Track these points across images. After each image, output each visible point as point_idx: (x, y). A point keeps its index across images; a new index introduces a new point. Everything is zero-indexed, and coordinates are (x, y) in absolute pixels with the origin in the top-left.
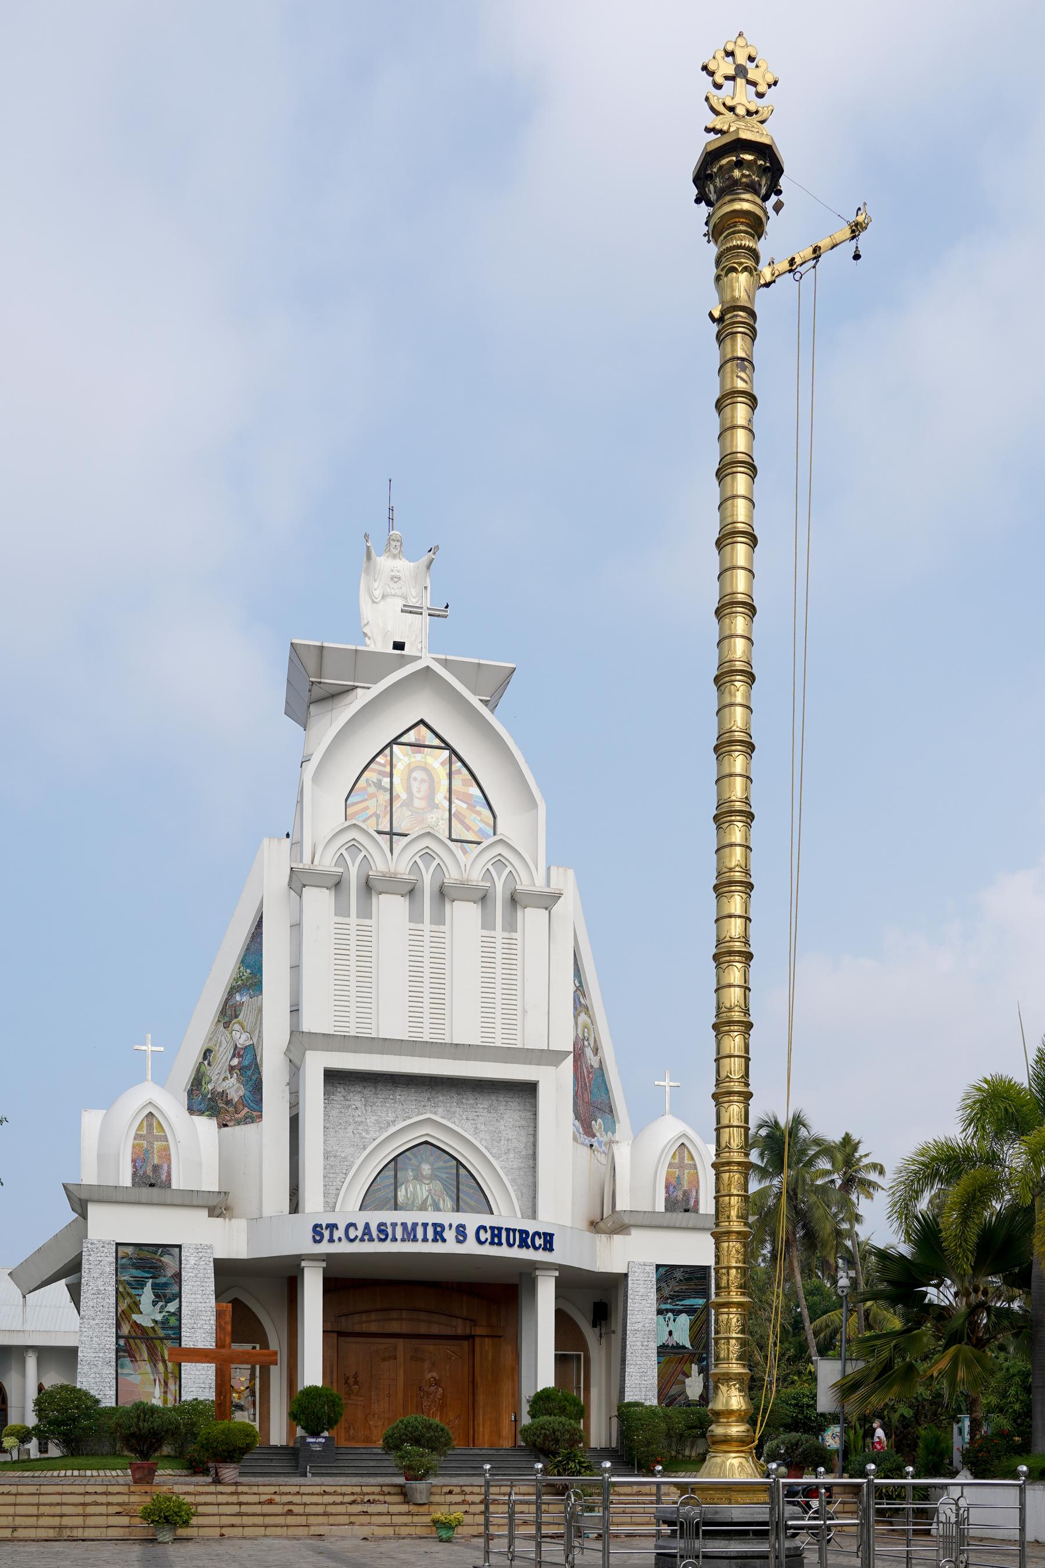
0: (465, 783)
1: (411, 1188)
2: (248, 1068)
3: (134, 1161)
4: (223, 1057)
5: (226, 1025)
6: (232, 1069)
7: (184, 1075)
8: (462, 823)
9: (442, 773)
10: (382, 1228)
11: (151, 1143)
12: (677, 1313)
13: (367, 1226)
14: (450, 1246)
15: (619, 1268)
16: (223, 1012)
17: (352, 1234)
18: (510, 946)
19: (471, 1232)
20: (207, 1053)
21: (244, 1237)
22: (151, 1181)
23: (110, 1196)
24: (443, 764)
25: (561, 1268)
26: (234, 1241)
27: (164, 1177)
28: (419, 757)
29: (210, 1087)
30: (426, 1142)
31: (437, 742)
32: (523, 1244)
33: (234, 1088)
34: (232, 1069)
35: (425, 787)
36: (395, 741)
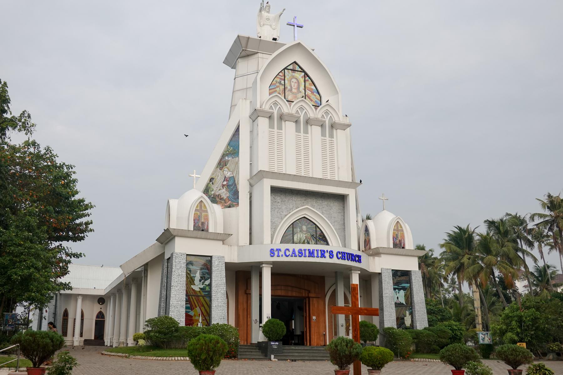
0: (310, 84)
1: (299, 235)
2: (231, 185)
3: (194, 220)
4: (219, 181)
5: (221, 169)
6: (223, 186)
7: (203, 187)
8: (309, 98)
9: (302, 80)
10: (300, 251)
11: (201, 213)
13: (294, 250)
14: (327, 260)
16: (219, 163)
17: (288, 253)
20: (211, 180)
21: (236, 253)
22: (200, 228)
23: (184, 234)
24: (302, 77)
27: (206, 227)
28: (294, 74)
29: (213, 193)
30: (304, 217)
31: (300, 70)
33: (224, 194)
34: (223, 186)
35: (296, 85)
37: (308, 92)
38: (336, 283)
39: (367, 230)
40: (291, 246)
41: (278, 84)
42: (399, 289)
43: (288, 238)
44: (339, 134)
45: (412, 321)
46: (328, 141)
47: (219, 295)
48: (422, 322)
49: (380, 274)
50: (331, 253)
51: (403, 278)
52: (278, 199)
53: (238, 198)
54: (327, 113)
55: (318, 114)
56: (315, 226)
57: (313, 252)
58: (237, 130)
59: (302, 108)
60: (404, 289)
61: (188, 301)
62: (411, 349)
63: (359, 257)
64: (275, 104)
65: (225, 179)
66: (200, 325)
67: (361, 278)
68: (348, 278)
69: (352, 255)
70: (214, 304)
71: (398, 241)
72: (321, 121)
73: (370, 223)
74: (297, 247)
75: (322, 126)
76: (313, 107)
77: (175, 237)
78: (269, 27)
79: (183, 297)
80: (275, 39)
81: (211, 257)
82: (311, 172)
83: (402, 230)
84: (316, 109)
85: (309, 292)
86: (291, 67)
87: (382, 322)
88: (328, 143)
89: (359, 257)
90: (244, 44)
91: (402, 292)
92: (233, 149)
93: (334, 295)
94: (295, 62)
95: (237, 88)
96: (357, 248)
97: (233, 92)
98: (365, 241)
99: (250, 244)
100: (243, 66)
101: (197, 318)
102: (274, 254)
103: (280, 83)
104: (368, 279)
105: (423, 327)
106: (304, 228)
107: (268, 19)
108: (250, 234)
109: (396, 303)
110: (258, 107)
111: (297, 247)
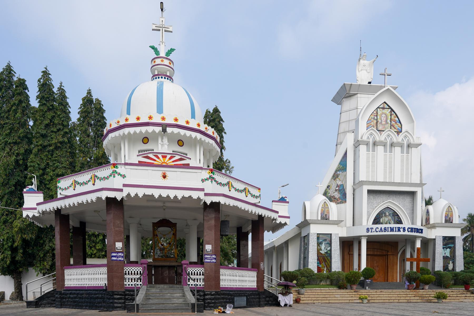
0: (394, 117)
8: (394, 127)
9: (389, 114)
10: (385, 229)
13: (381, 228)
14: (402, 233)
19: (406, 229)
22: (325, 218)
23: (316, 222)
28: (384, 111)
31: (388, 107)
35: (385, 118)
37: (393, 123)
38: (405, 246)
39: (428, 212)
40: (379, 226)
41: (372, 120)
42: (447, 248)
43: (377, 221)
44: (414, 150)
45: (454, 267)
46: (405, 156)
47: (336, 255)
48: (460, 266)
49: (435, 239)
50: (404, 229)
51: (450, 241)
52: (372, 197)
53: (346, 198)
54: (406, 137)
55: (400, 138)
57: (393, 229)
58: (346, 154)
59: (389, 136)
60: (450, 248)
61: (318, 259)
62: (451, 283)
63: (422, 230)
64: (371, 134)
65: (338, 186)
66: (325, 272)
67: (422, 242)
68: (413, 243)
70: (333, 260)
72: (402, 143)
73: (430, 207)
74: (383, 226)
75: (401, 146)
76: (395, 133)
77: (309, 224)
78: (365, 71)
79: (316, 257)
80: (370, 83)
81: (331, 234)
82: (392, 180)
83: (452, 211)
84: (398, 134)
85: (388, 251)
86: (382, 106)
87: (434, 267)
88: (405, 157)
89: (422, 230)
90: (348, 88)
91: (448, 250)
92: (343, 166)
93: (404, 253)
94: (385, 102)
95: (342, 121)
96: (420, 225)
97: (340, 123)
98: (426, 219)
99: (353, 225)
100: (348, 104)
101: (323, 268)
102: (369, 231)
103: (374, 118)
104: (426, 243)
105: (460, 270)
106: (387, 214)
107: (364, 66)
108: (353, 218)
109: (443, 257)
110: (360, 139)
111: (383, 226)
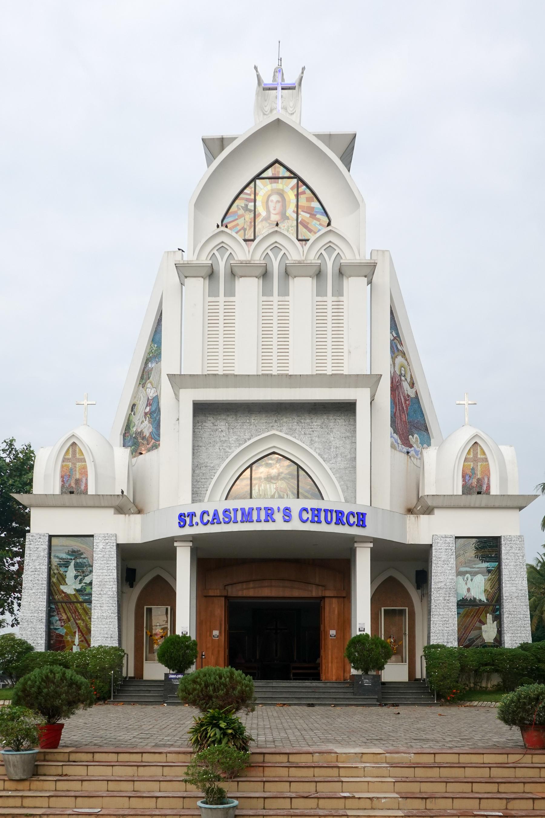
0: (308, 200)
1: (262, 487)
2: (154, 412)
3: (62, 477)
4: (142, 408)
6: (146, 414)
8: (306, 227)
9: (291, 196)
12: (474, 574)
13: (216, 513)
14: (279, 525)
15: (424, 540)
17: (206, 518)
18: (338, 307)
19: (295, 514)
24: (292, 189)
25: (375, 541)
26: (133, 531)
27: (83, 487)
29: (134, 429)
30: (274, 453)
31: (288, 174)
32: (339, 522)
33: (146, 428)
34: (146, 414)
35: (279, 206)
36: (258, 177)
41: (241, 212)
56: (296, 466)
69: (339, 513)
71: (474, 482)
94: (277, 162)
103: (246, 208)
